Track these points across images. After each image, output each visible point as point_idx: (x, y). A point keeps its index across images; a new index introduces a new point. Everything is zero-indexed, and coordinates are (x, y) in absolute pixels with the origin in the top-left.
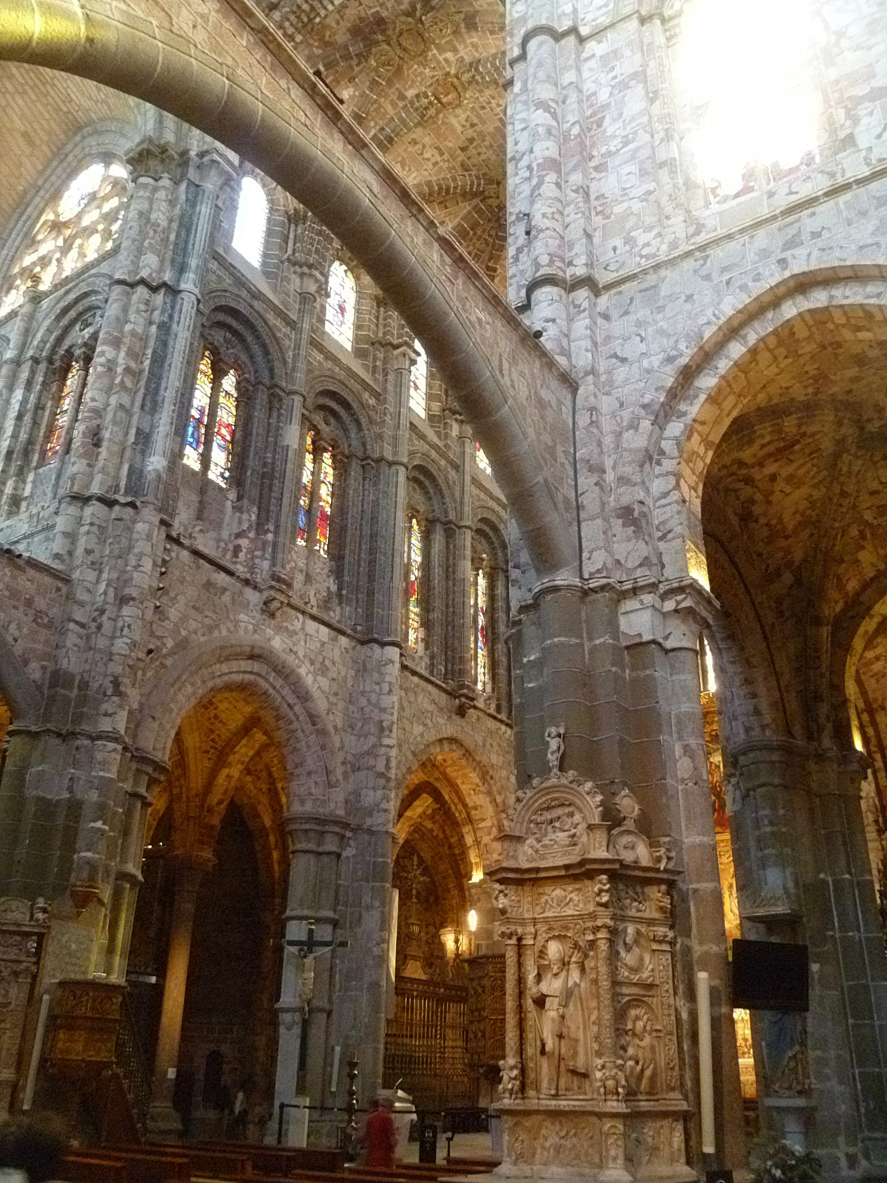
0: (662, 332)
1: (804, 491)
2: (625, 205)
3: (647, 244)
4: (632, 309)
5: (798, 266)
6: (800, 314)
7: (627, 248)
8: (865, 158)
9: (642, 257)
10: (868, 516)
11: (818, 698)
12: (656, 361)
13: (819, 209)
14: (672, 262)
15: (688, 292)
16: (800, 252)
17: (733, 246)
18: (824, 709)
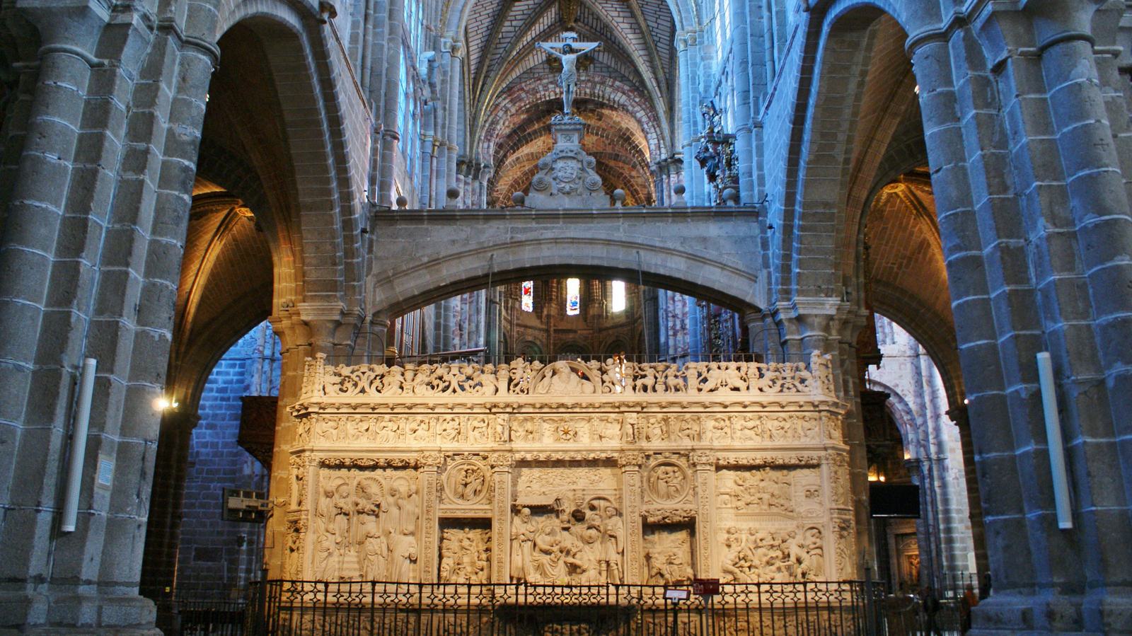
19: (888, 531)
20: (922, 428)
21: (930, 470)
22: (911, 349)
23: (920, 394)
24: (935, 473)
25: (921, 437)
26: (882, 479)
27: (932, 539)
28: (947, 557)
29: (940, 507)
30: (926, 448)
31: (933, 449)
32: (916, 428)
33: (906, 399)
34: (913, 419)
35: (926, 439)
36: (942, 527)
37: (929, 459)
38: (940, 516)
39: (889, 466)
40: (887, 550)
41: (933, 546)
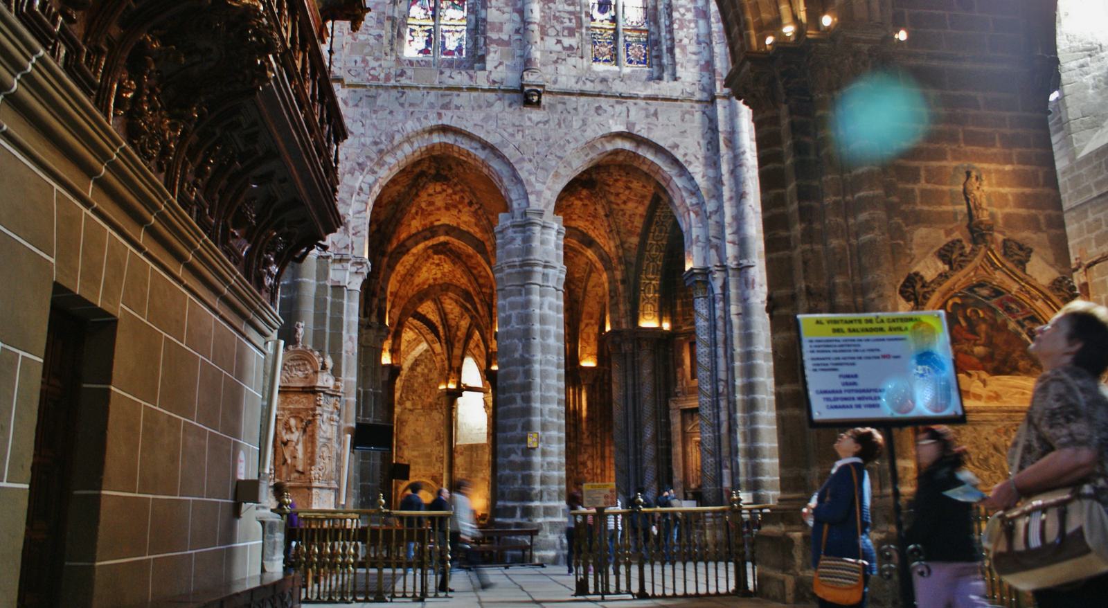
0: (374, 126)
1: (398, 187)
2: (366, 36)
3: (374, 69)
4: (360, 104)
5: (446, 121)
6: (440, 143)
7: (363, 65)
8: (488, 76)
9: (370, 75)
10: (423, 205)
11: (374, 295)
12: (368, 141)
13: (462, 94)
14: (386, 88)
15: (391, 109)
16: (449, 113)
17: (418, 93)
18: (376, 301)
19: (672, 405)
20: (714, 218)
21: (725, 287)
22: (703, 90)
23: (713, 161)
24: (733, 292)
25: (712, 232)
26: (666, 326)
27: (723, 404)
28: (744, 434)
29: (738, 349)
30: (720, 250)
31: (730, 251)
32: (704, 216)
33: (690, 169)
34: (701, 204)
35: (721, 236)
36: (739, 382)
37: (724, 268)
38: (737, 364)
39: (679, 309)
40: (668, 434)
41: (724, 416)
